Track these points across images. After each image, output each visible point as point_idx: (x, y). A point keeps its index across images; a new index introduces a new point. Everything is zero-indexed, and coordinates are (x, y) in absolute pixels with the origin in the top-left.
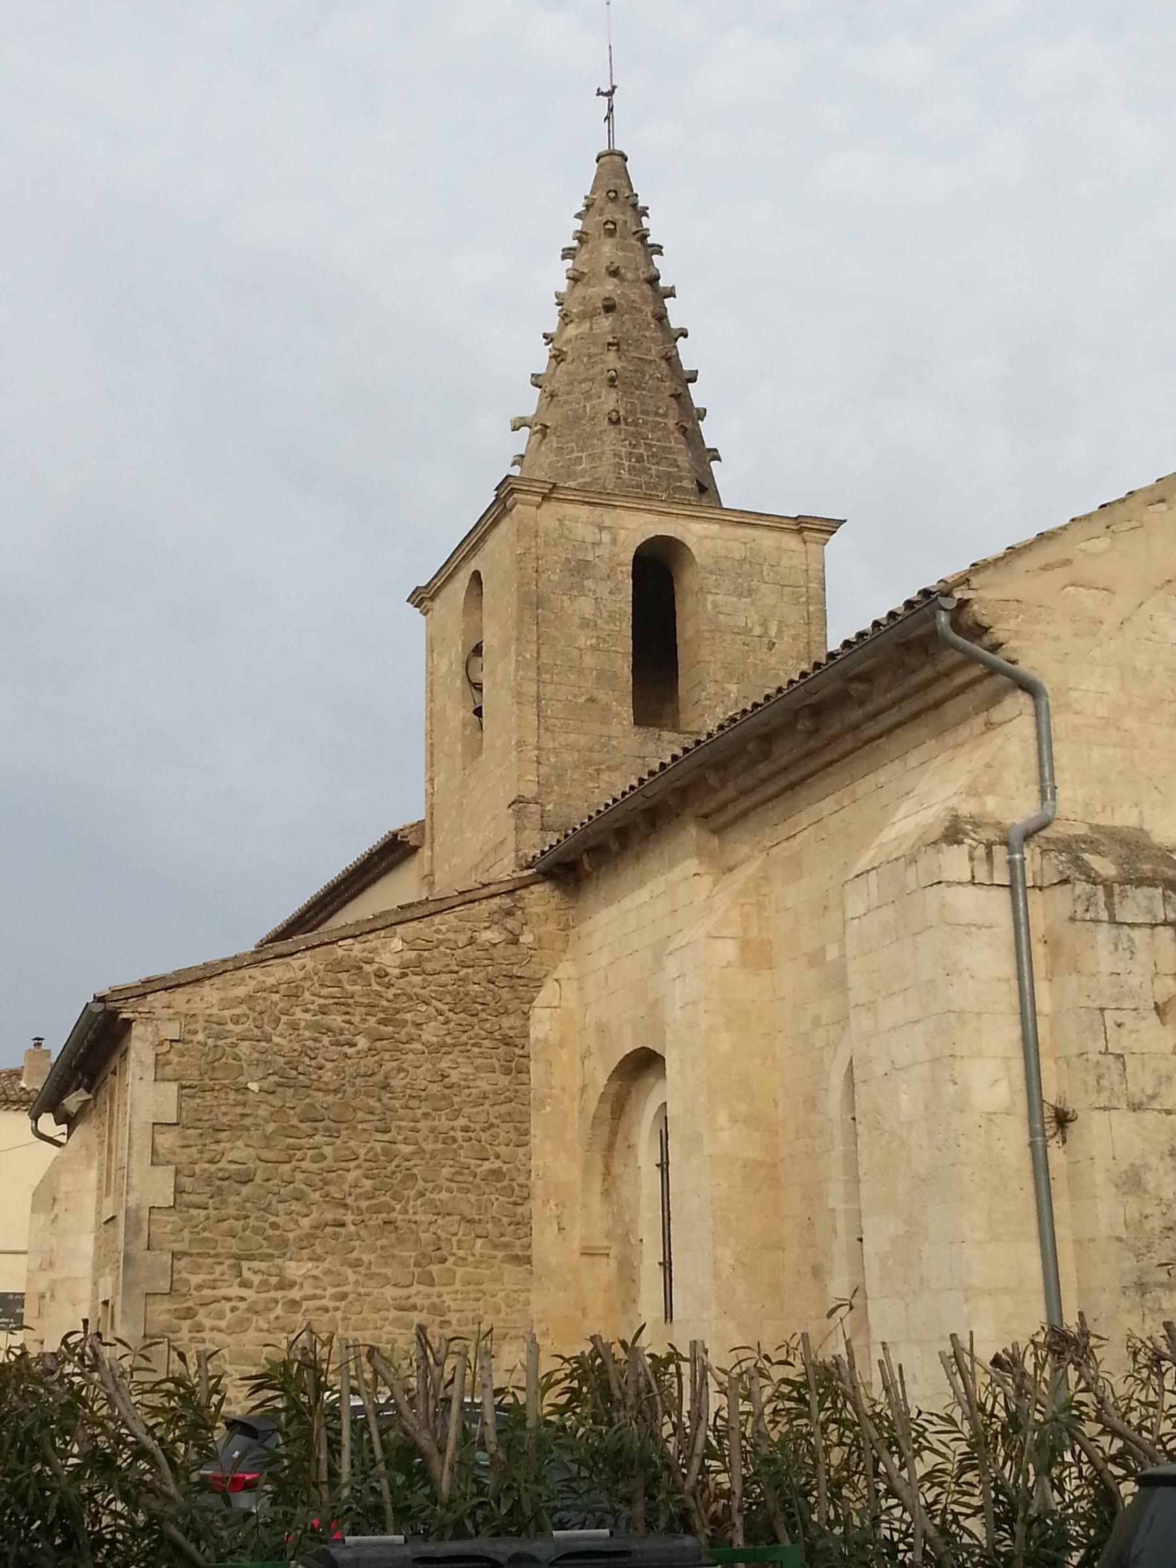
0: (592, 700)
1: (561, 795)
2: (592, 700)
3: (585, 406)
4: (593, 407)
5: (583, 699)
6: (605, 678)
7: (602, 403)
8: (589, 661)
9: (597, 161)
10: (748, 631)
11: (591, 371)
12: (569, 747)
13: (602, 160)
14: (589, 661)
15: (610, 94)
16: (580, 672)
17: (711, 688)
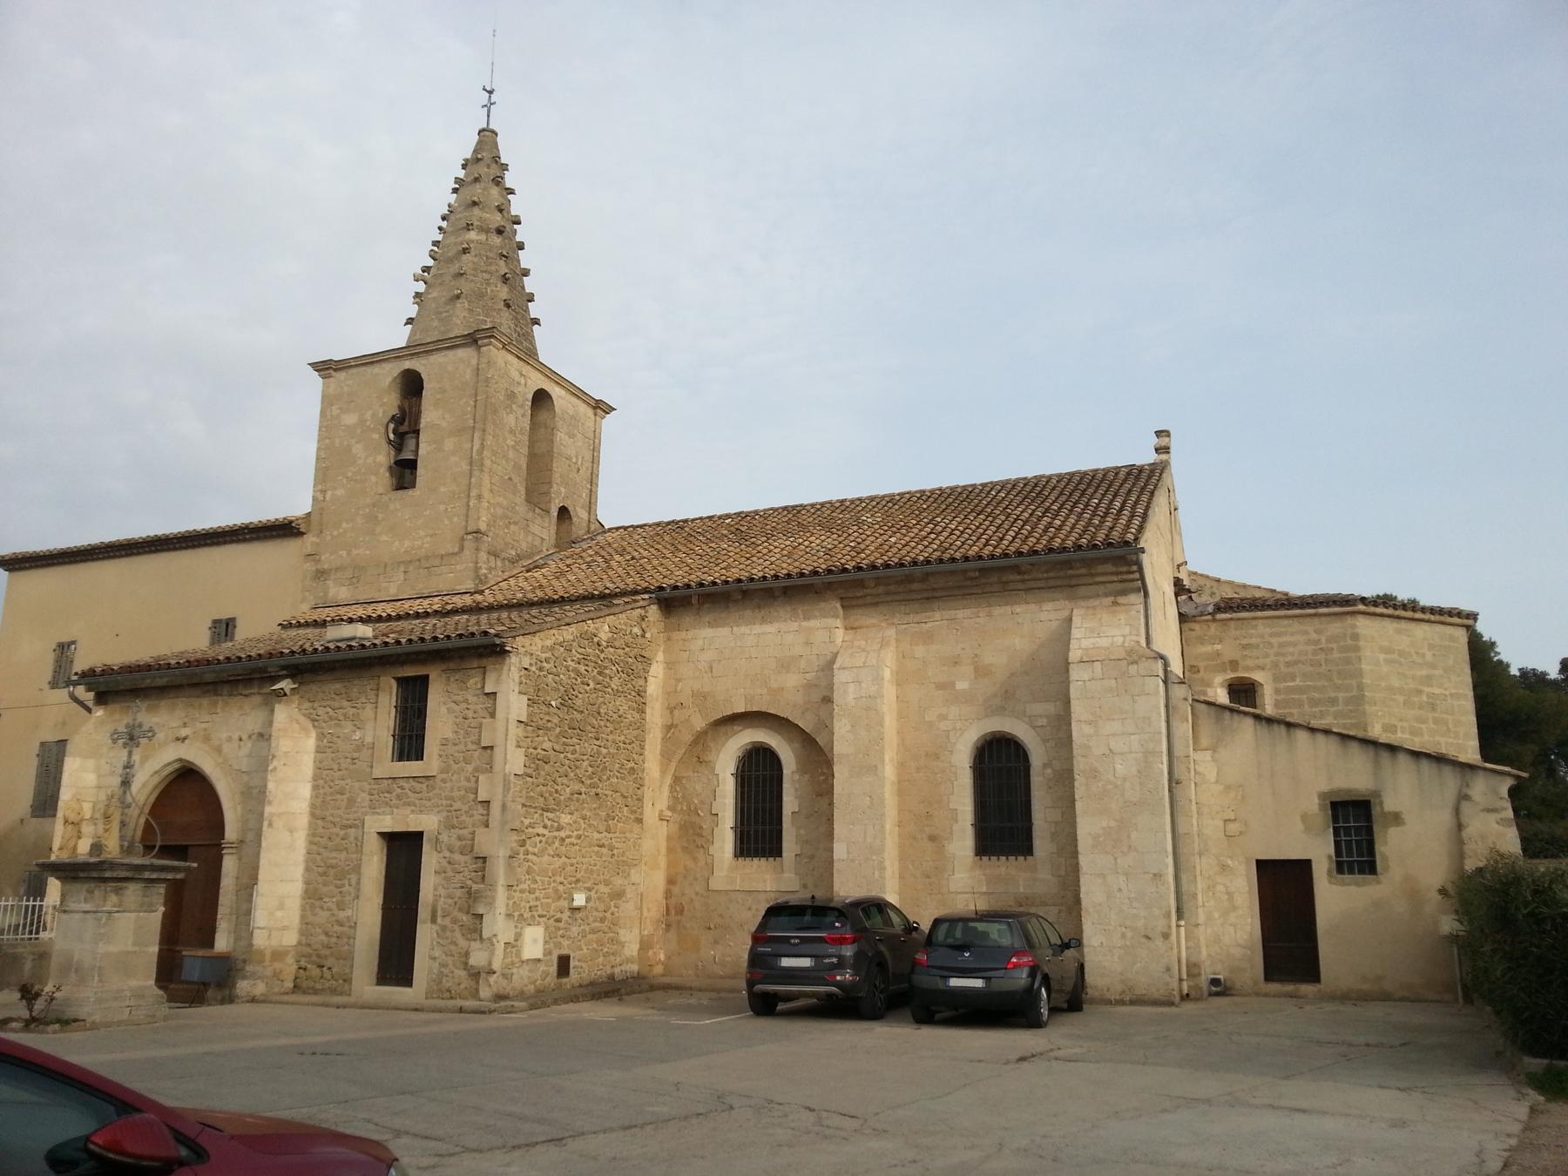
0: (510, 479)
1: (494, 533)
2: (510, 479)
3: (486, 289)
4: (492, 291)
5: (506, 478)
6: (517, 467)
7: (498, 291)
8: (511, 454)
9: (480, 132)
10: (569, 459)
11: (489, 268)
12: (500, 505)
13: (482, 134)
14: (511, 454)
15: (490, 92)
16: (507, 460)
17: (555, 487)
